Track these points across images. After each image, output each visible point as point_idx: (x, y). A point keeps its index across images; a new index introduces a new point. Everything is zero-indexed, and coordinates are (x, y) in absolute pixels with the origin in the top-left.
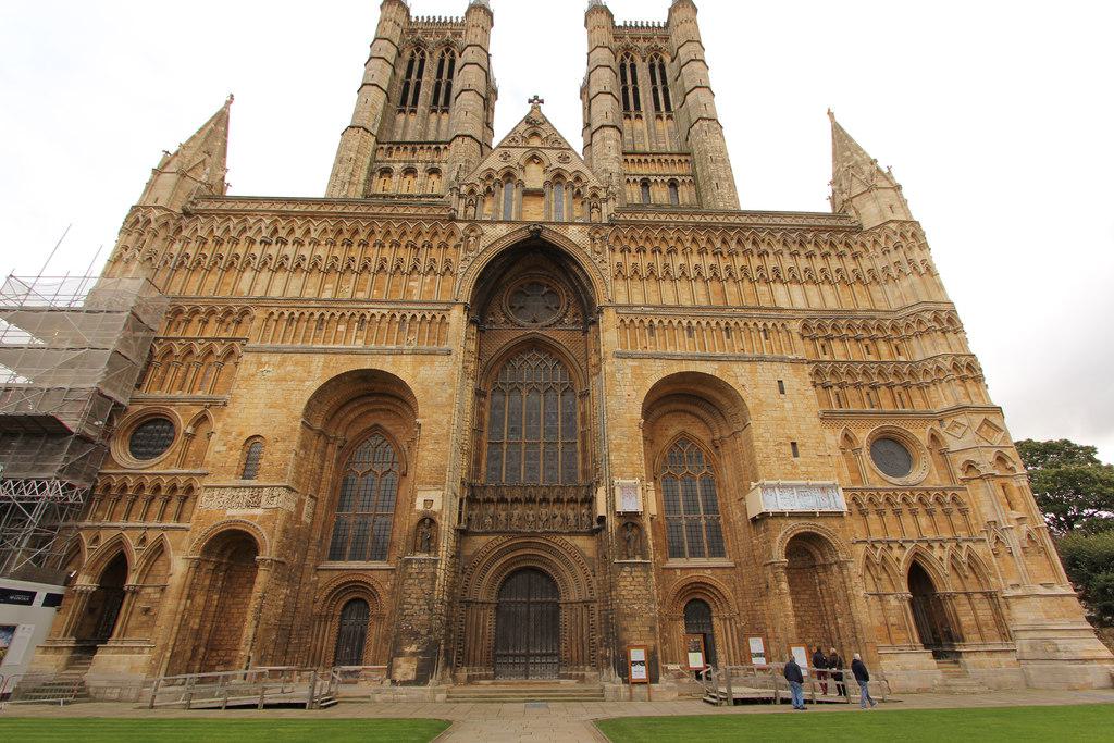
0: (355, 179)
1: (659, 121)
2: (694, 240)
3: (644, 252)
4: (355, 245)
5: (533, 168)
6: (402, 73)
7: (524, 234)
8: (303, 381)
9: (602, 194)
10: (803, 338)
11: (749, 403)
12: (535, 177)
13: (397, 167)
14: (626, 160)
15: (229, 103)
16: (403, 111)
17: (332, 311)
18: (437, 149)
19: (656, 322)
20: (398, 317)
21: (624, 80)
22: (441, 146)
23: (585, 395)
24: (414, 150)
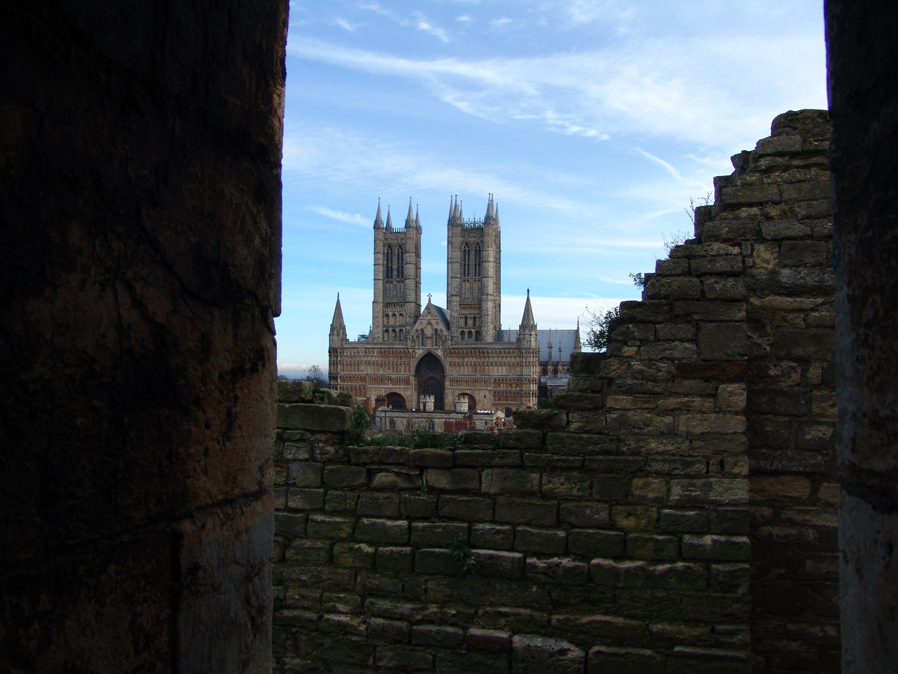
2: (471, 352)
5: (429, 326)
6: (385, 262)
7: (425, 353)
9: (448, 337)
10: (494, 383)
11: (477, 401)
13: (390, 314)
15: (338, 296)
24: (394, 305)
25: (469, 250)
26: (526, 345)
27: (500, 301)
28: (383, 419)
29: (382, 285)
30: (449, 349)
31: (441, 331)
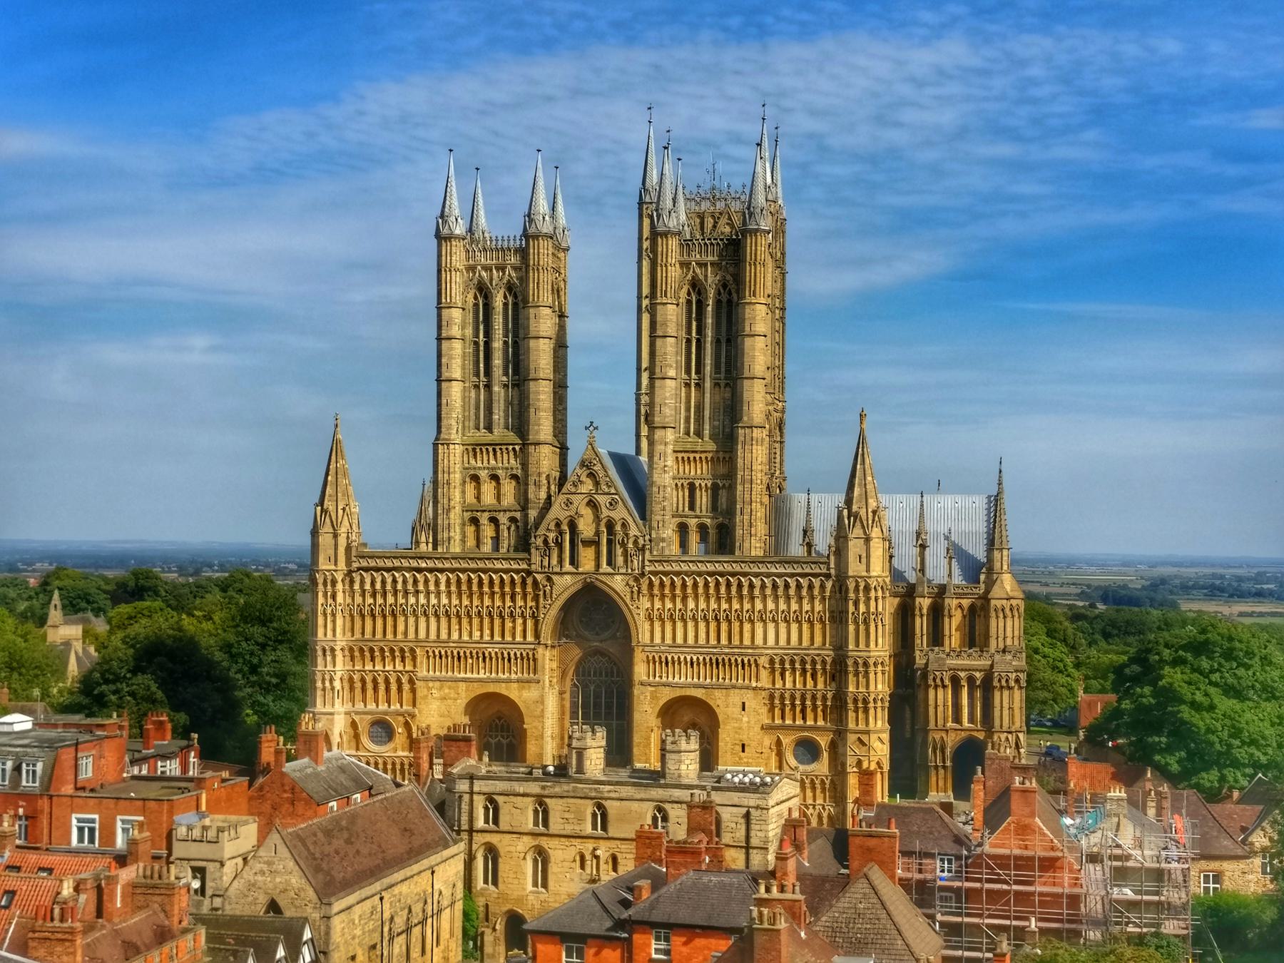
6: (469, 331)
8: (456, 699)
9: (641, 541)
11: (721, 718)
13: (483, 474)
19: (670, 658)
20: (506, 655)
22: (517, 448)
26: (854, 568)
27: (783, 411)
28: (466, 798)
29: (459, 395)
30: (643, 574)
31: (624, 525)
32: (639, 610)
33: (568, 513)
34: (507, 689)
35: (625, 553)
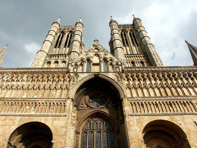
0: (38, 64)
1: (134, 47)
3: (136, 80)
4: (36, 81)
6: (56, 39)
7: (93, 76)
8: (11, 126)
9: (119, 63)
11: (184, 131)
12: (96, 60)
13: (53, 61)
14: (126, 57)
16: (56, 48)
17: (25, 102)
18: (66, 56)
19: (143, 103)
21: (122, 37)
22: (67, 55)
23: (118, 132)
24: (58, 56)
25: (125, 34)
30: (123, 72)
31: (111, 60)
32: (123, 85)
33: (86, 57)
34: (45, 120)
35: (113, 67)
